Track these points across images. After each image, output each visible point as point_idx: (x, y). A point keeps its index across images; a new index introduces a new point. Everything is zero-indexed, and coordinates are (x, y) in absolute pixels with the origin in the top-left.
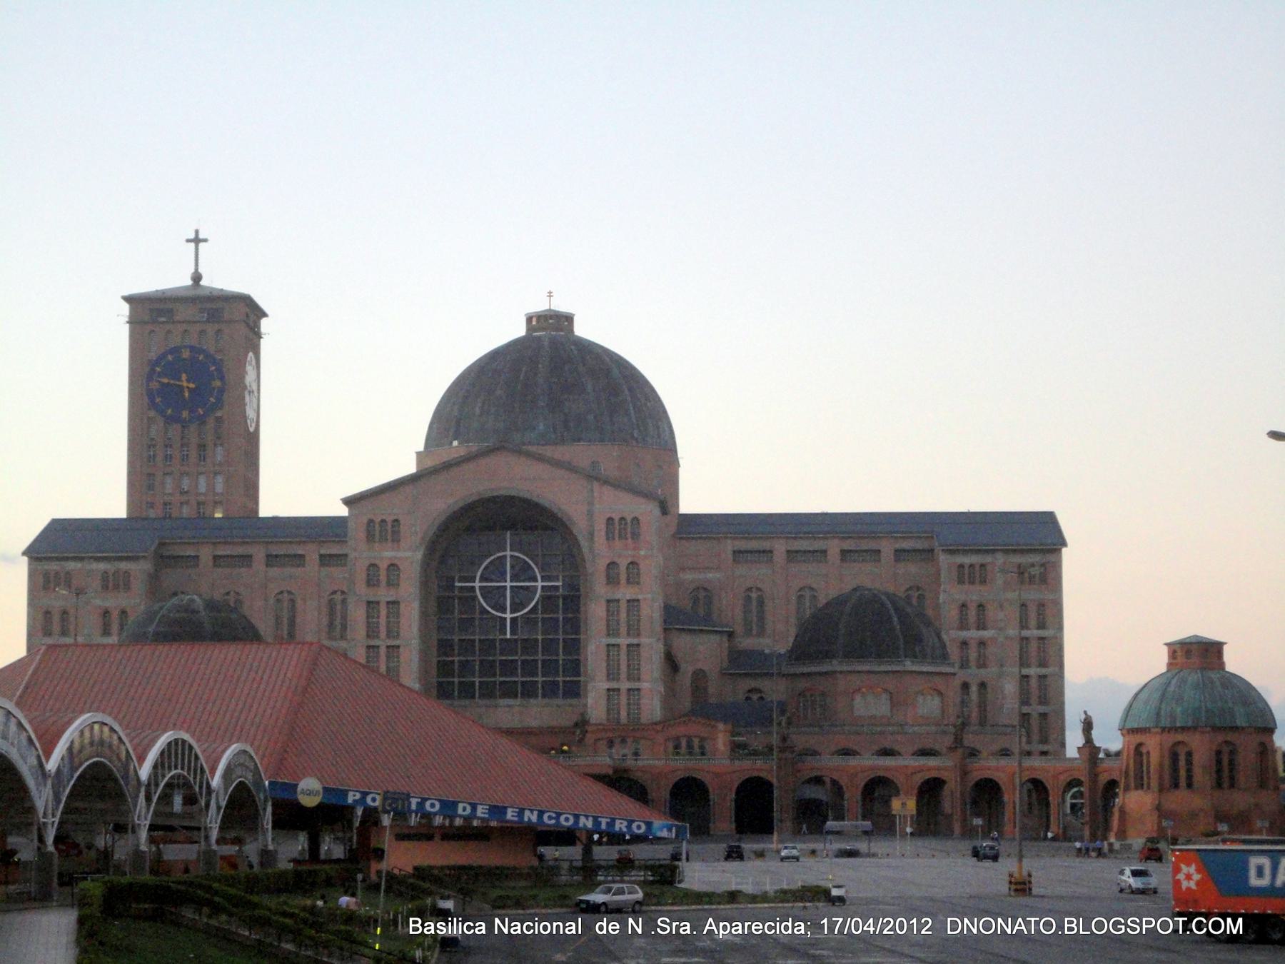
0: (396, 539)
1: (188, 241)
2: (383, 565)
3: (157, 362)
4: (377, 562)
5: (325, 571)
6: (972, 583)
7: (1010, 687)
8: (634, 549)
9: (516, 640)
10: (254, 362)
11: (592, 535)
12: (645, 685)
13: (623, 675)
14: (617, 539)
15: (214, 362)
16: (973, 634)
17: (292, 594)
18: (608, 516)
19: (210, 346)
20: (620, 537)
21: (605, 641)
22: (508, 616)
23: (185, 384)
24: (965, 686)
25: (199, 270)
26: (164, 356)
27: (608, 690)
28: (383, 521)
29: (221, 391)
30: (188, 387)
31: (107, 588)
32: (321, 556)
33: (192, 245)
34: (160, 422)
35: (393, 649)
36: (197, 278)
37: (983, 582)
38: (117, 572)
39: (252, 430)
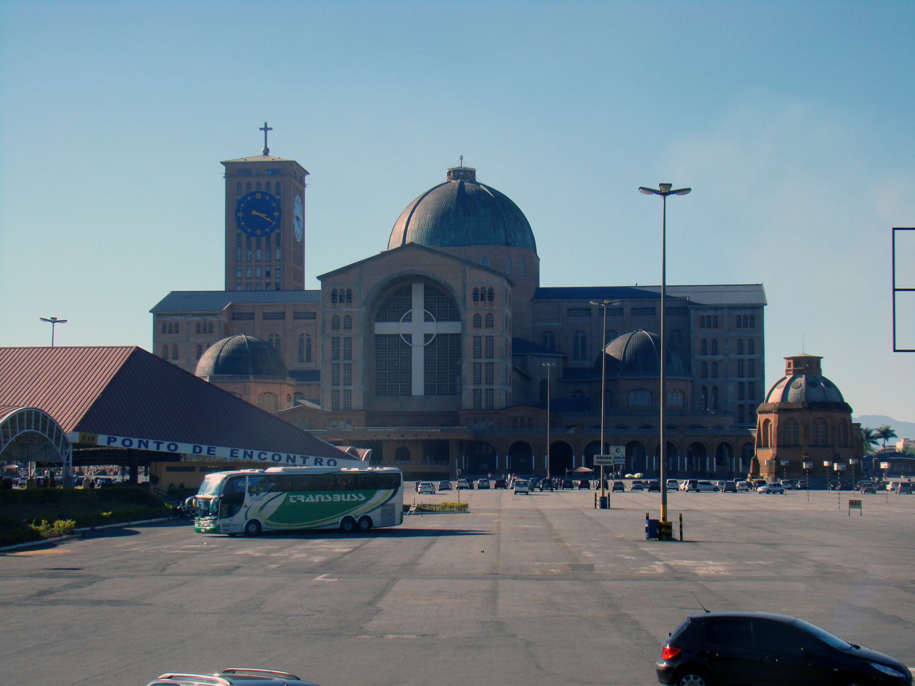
1: (261, 129)
2: (342, 316)
6: (709, 327)
7: (732, 390)
10: (300, 201)
12: (496, 387)
13: (483, 381)
14: (480, 299)
16: (708, 357)
17: (309, 335)
18: (474, 287)
19: (273, 193)
20: (482, 299)
21: (473, 360)
24: (705, 389)
25: (268, 147)
26: (246, 197)
27: (475, 390)
28: (342, 290)
34: (244, 235)
36: (266, 152)
37: (716, 326)
39: (299, 241)
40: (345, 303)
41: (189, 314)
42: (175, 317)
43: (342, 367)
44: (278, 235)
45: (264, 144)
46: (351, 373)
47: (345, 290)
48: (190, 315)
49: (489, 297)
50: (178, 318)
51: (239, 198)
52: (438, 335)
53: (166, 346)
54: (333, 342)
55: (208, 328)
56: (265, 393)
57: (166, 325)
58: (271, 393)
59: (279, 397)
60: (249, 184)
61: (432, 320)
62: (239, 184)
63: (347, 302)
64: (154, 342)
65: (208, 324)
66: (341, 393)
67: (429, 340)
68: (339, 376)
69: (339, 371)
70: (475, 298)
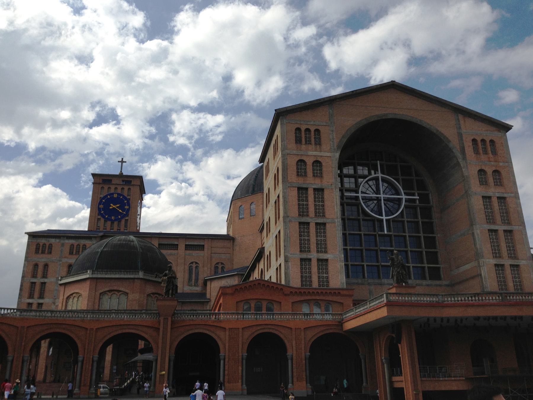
0: (318, 142)
2: (309, 161)
3: (103, 198)
5: (188, 252)
8: (496, 161)
9: (390, 236)
18: (472, 138)
19: (125, 193)
22: (384, 218)
23: (114, 206)
26: (106, 196)
27: (496, 265)
28: (308, 130)
31: (73, 253)
32: (186, 245)
33: (120, 163)
34: (102, 220)
35: (321, 226)
38: (79, 245)
40: (313, 146)
41: (64, 236)
45: (120, 170)
47: (313, 129)
48: (65, 238)
50: (52, 241)
51: (102, 196)
53: (36, 265)
54: (298, 194)
56: (153, 294)
57: (39, 247)
63: (316, 144)
65: (81, 246)
66: (314, 263)
68: (309, 240)
69: (308, 232)
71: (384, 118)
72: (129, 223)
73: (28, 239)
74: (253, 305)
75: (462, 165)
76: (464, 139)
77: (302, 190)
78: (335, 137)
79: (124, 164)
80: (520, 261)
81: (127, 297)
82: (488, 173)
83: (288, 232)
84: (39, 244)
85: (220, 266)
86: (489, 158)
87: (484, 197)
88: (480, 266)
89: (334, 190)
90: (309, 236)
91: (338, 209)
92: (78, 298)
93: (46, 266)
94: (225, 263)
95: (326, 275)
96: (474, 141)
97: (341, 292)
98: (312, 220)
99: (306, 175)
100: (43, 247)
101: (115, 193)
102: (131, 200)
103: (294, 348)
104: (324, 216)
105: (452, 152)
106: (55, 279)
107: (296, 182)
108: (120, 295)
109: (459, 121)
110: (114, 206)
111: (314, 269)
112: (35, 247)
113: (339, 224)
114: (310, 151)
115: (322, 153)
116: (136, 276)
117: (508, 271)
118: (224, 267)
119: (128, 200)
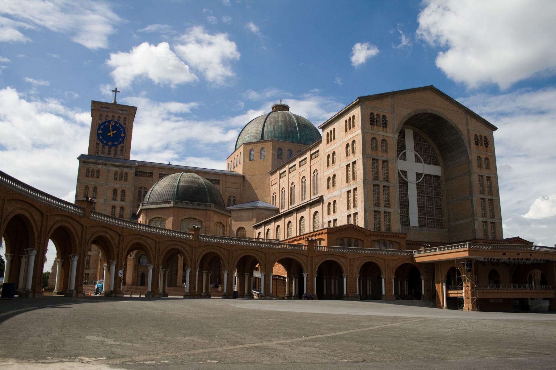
2: (379, 139)
3: (102, 124)
4: (376, 137)
11: (469, 141)
15: (122, 127)
18: (475, 133)
19: (122, 123)
23: (111, 133)
26: (105, 123)
27: (483, 222)
29: (124, 137)
30: (111, 134)
31: (117, 179)
33: (114, 93)
34: (101, 145)
36: (115, 102)
38: (122, 172)
41: (109, 164)
42: (98, 166)
43: (381, 188)
44: (122, 147)
46: (389, 196)
47: (381, 115)
48: (110, 165)
49: (485, 144)
50: (100, 167)
51: (100, 122)
52: (426, 175)
53: (87, 187)
55: (123, 177)
56: (218, 223)
58: (221, 224)
59: (226, 228)
60: (107, 116)
61: (421, 162)
62: (101, 115)
63: (383, 127)
64: (78, 182)
66: (382, 214)
67: (419, 179)
70: (477, 143)
71: (425, 112)
72: (124, 149)
73: (79, 164)
74: (346, 242)
75: (468, 152)
76: (470, 133)
77: (375, 160)
78: (395, 123)
79: (117, 93)
80: (495, 220)
81: (201, 224)
82: (482, 159)
83: (367, 190)
84: (89, 169)
85: (232, 199)
86: (483, 149)
87: (479, 176)
88: (474, 222)
89: (395, 162)
90: (378, 194)
91: (397, 177)
92: (161, 222)
93: (95, 188)
94: (236, 197)
95: (389, 223)
96: (476, 135)
97: (400, 236)
98: (382, 184)
99: (376, 149)
100: (92, 171)
101: (113, 121)
102: (127, 128)
103: (387, 272)
104: (388, 181)
105: (464, 142)
106: (103, 200)
107: (370, 154)
108: (196, 222)
109: (468, 120)
110: (111, 133)
111: (382, 219)
112: (85, 172)
113: (397, 187)
114: (380, 132)
115: (387, 134)
116: (209, 208)
117: (489, 225)
118: (235, 200)
119: (124, 128)
